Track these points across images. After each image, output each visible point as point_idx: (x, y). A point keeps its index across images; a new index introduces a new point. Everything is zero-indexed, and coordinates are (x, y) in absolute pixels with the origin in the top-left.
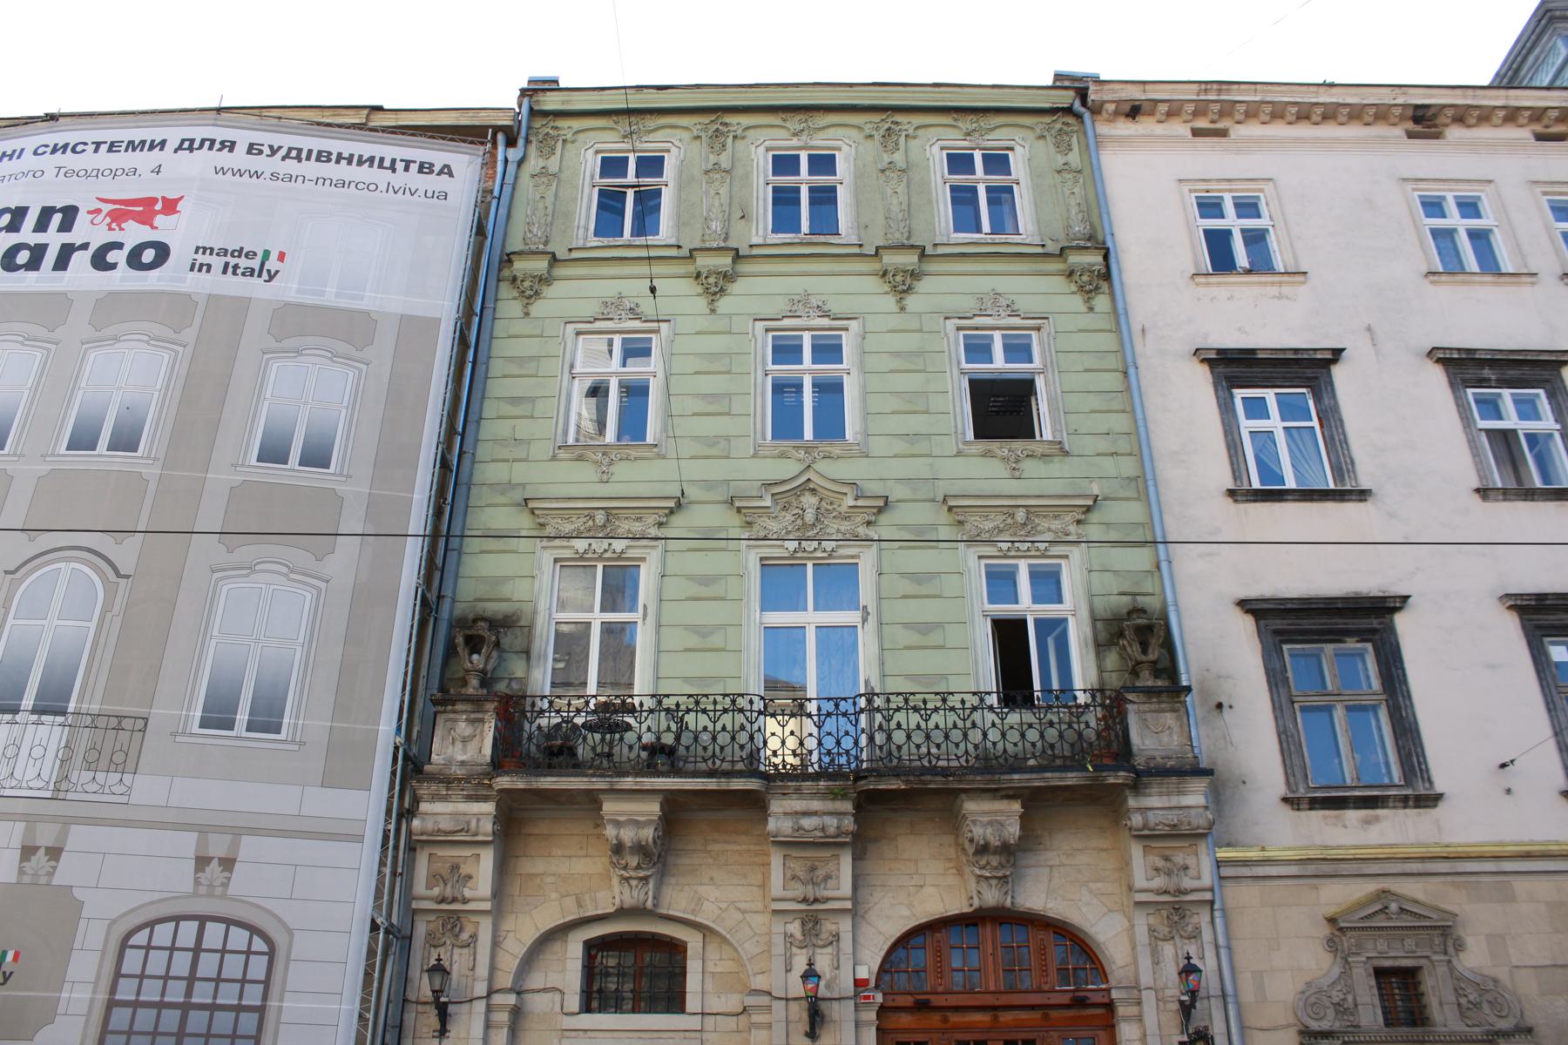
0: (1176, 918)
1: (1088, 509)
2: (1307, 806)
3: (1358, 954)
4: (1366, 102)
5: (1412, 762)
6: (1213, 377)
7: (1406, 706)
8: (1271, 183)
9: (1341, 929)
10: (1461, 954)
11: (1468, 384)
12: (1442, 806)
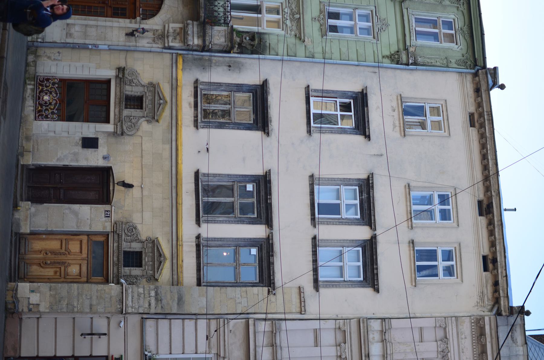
0: (160, 36)
1: (300, 39)
2: (195, 86)
3: (147, 90)
6: (356, 92)
7: (229, 127)
8: (448, 135)
11: (360, 187)
12: (195, 128)
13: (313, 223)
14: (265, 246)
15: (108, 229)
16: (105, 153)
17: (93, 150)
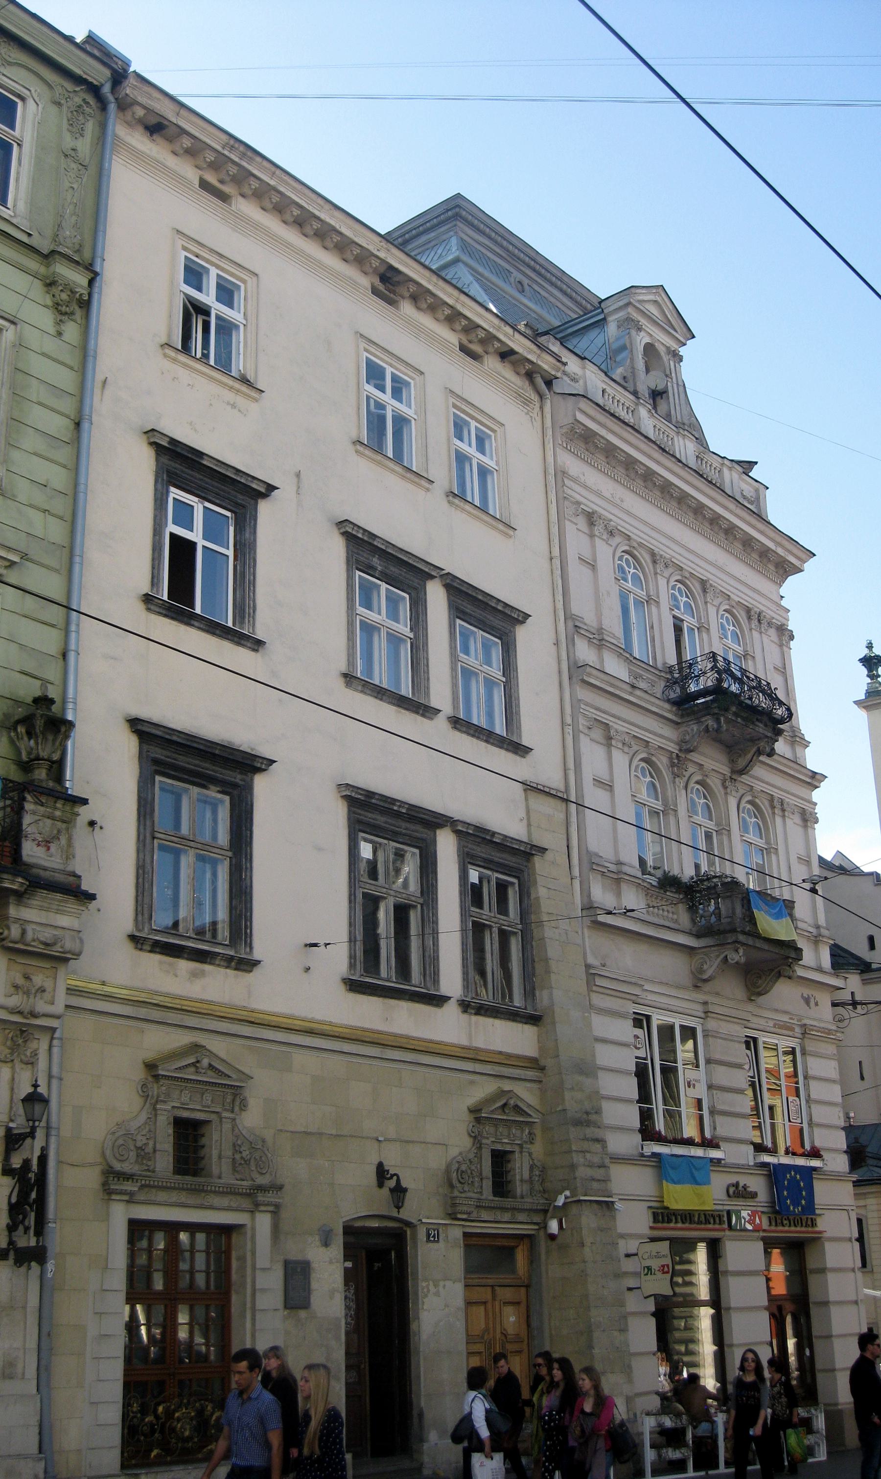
2: (149, 948)
3: (165, 1102)
4: (356, 240)
5: (240, 925)
6: (157, 465)
8: (255, 279)
9: (157, 1077)
10: (243, 1113)
12: (257, 971)
13: (431, 716)
14: (470, 846)
15: (456, 1233)
16: (316, 1240)
17: (313, 1276)
